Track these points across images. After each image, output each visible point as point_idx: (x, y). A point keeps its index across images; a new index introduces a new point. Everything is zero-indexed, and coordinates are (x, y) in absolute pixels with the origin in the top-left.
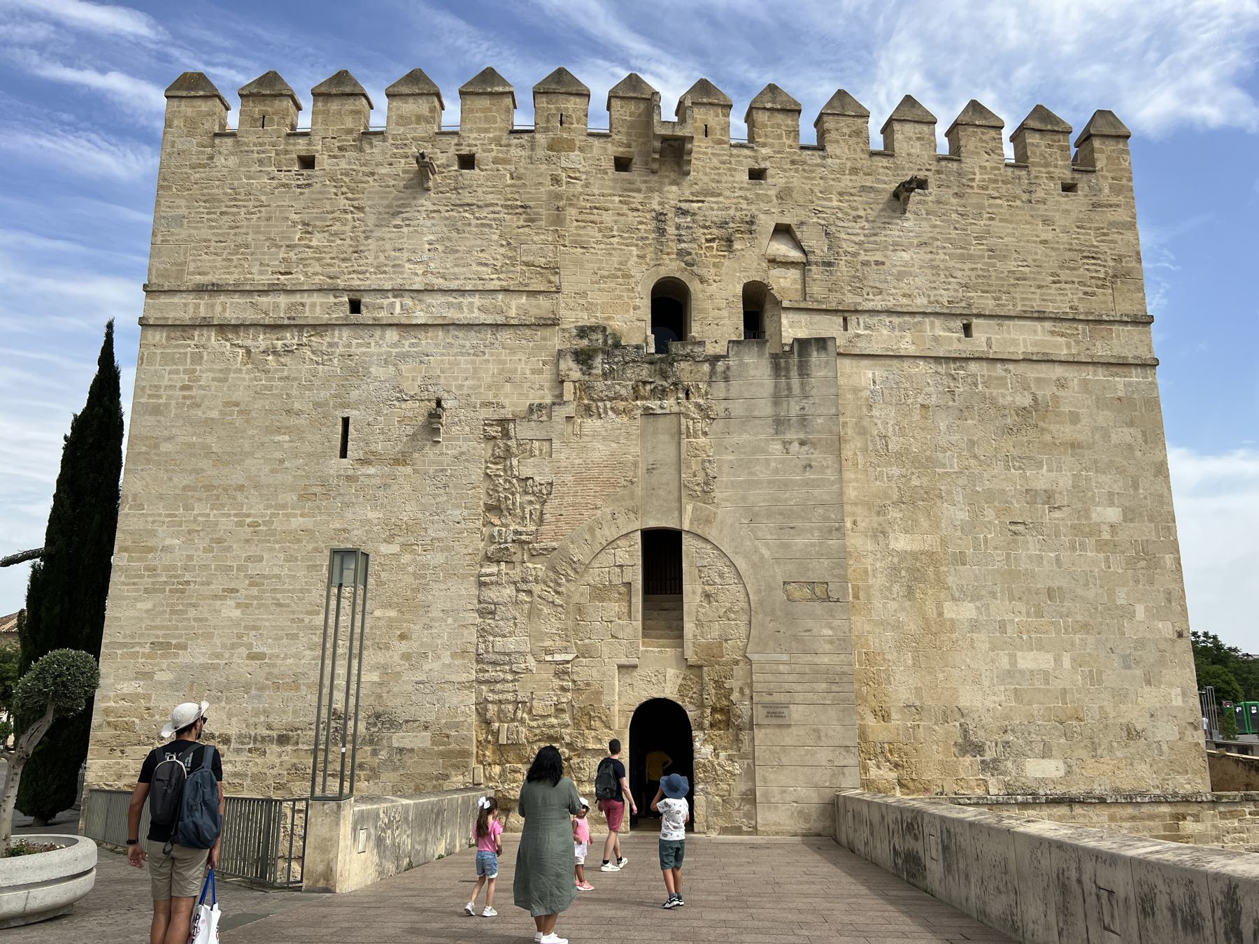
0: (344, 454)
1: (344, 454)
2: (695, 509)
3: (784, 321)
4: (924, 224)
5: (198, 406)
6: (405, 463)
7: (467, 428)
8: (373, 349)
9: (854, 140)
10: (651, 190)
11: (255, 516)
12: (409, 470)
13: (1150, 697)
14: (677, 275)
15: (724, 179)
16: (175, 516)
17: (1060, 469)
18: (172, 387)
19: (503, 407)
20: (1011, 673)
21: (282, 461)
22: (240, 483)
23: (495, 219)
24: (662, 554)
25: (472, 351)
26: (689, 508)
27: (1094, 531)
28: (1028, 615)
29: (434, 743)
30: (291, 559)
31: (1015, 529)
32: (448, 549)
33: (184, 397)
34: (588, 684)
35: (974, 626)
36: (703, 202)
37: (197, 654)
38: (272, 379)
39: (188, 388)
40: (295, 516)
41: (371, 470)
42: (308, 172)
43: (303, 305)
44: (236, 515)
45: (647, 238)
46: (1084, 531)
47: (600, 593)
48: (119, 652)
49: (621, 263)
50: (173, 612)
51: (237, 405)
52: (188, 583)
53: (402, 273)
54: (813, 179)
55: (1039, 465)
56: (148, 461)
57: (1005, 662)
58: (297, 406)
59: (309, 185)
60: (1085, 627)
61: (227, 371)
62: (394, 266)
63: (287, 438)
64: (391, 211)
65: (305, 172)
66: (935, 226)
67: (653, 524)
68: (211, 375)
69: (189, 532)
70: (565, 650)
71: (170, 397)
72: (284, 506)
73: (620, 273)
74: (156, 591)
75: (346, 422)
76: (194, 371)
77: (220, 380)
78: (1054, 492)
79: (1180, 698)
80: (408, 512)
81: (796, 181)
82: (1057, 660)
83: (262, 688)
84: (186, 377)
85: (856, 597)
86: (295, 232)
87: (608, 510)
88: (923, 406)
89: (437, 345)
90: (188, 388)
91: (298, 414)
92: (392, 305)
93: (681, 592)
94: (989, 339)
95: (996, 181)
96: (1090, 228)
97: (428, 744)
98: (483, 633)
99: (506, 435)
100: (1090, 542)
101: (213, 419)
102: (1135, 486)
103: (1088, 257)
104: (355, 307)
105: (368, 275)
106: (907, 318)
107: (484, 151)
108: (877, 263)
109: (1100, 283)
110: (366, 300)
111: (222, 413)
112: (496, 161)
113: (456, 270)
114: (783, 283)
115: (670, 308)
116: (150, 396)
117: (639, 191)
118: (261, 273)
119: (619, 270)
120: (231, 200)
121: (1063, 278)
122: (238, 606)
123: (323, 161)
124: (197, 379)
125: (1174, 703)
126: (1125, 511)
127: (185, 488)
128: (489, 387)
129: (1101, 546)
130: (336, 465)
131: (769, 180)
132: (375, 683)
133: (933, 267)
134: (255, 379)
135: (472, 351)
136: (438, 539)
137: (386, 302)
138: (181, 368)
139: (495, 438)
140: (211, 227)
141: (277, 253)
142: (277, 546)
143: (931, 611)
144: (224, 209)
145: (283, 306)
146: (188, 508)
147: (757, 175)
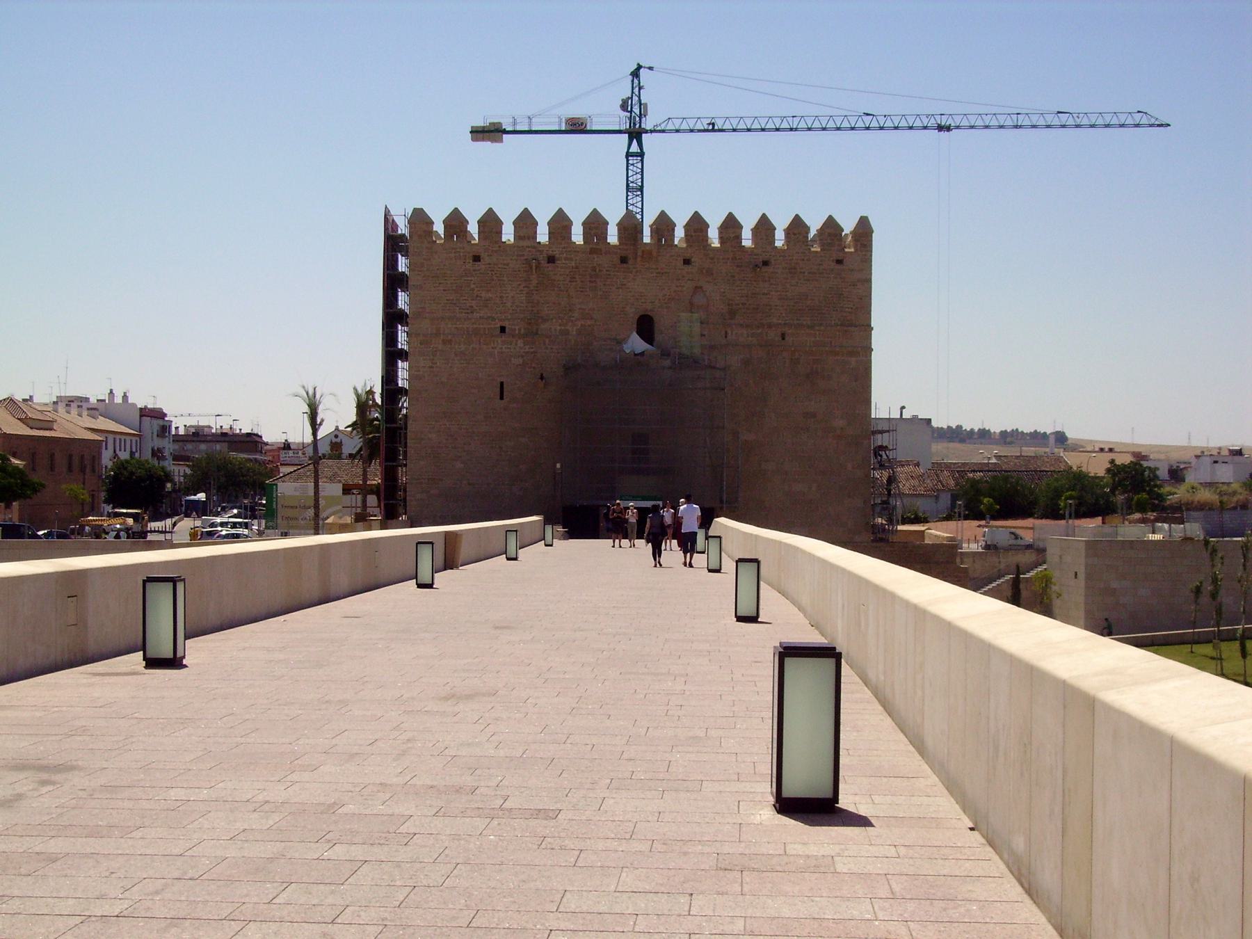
0: (502, 398)
1: (502, 398)
75: (502, 384)
104: (503, 329)
112: (566, 259)
123: (486, 259)
147: (687, 262)
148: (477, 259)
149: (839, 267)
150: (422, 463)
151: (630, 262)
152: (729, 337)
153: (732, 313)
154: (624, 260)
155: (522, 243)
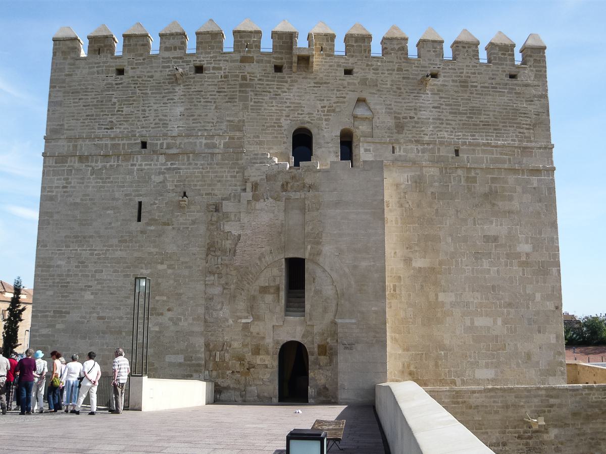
0: (139, 220)
1: (139, 220)
2: (312, 248)
3: (362, 150)
4: (437, 97)
5: (70, 196)
6: (168, 225)
7: (199, 207)
8: (152, 167)
9: (400, 52)
10: (292, 81)
11: (99, 250)
12: (171, 227)
13: (539, 339)
14: (307, 126)
15: (331, 75)
16: (61, 250)
17: (501, 225)
18: (58, 187)
19: (216, 195)
20: (471, 329)
21: (110, 223)
22: (91, 234)
23: (213, 99)
24: (296, 271)
25: (201, 167)
26: (309, 247)
27: (518, 255)
28: (482, 298)
29: (185, 360)
30: (115, 271)
31: (478, 256)
32: (190, 267)
33: (64, 192)
34: (258, 334)
35: (453, 305)
36: (320, 87)
37: (74, 316)
38: (105, 182)
39: (66, 187)
40: (117, 250)
41: (152, 228)
42: (121, 76)
43: (119, 144)
44: (89, 250)
45: (290, 107)
46: (512, 256)
47: (264, 290)
48: (39, 314)
49: (277, 119)
50: (62, 296)
51: (88, 195)
52: (68, 282)
53: (167, 127)
54: (378, 74)
55: (492, 222)
56: (49, 224)
57: (468, 323)
58: (117, 195)
59: (121, 83)
60: (510, 305)
61: (83, 179)
62: (163, 124)
63: (112, 212)
64: (162, 95)
65: (119, 77)
66: (441, 98)
67: (291, 255)
68: (75, 180)
69: (69, 258)
70: (247, 318)
71: (57, 192)
72: (112, 246)
73: (276, 125)
74: (54, 286)
75: (140, 203)
76: (68, 179)
77: (80, 183)
78: (498, 237)
79: (555, 339)
80: (171, 248)
81: (370, 75)
82: (495, 322)
83: (104, 333)
84: (65, 182)
85: (395, 290)
86: (115, 108)
87: (268, 248)
88: (432, 193)
89: (184, 164)
90: (66, 187)
91: (117, 199)
92: (162, 144)
93: (303, 288)
94: (468, 157)
95: (474, 73)
96: (523, 97)
97: (182, 361)
98: (207, 308)
99: (217, 210)
100: (515, 262)
101: (77, 203)
102: (540, 233)
103: (521, 113)
104: (144, 145)
105: (150, 129)
106: (426, 146)
107: (208, 63)
108: (411, 118)
109: (528, 127)
110: (149, 141)
111: (82, 200)
112: (214, 68)
113: (194, 125)
114: (361, 129)
115: (302, 144)
116: (48, 191)
117: (287, 82)
118: (99, 129)
119: (276, 123)
120: (84, 92)
121: (508, 124)
122: (92, 294)
123: (129, 72)
124: (70, 183)
125: (552, 342)
126: (534, 248)
127: (66, 237)
128: (210, 185)
129: (523, 264)
130: (135, 226)
131: (355, 75)
132: (156, 331)
133: (440, 119)
134: (97, 182)
135: (201, 167)
136: (186, 263)
137: (159, 142)
138: (62, 177)
139: (212, 211)
140: (75, 106)
141: (106, 119)
142: (109, 265)
143: (432, 296)
144: (80, 97)
145: (109, 146)
146: (67, 246)
147: (348, 72)
148: (121, 72)
149: (514, 81)
150: (51, 293)
151: (285, 70)
152: (397, 153)
153: (400, 127)
154: (278, 69)
155: (167, 54)
